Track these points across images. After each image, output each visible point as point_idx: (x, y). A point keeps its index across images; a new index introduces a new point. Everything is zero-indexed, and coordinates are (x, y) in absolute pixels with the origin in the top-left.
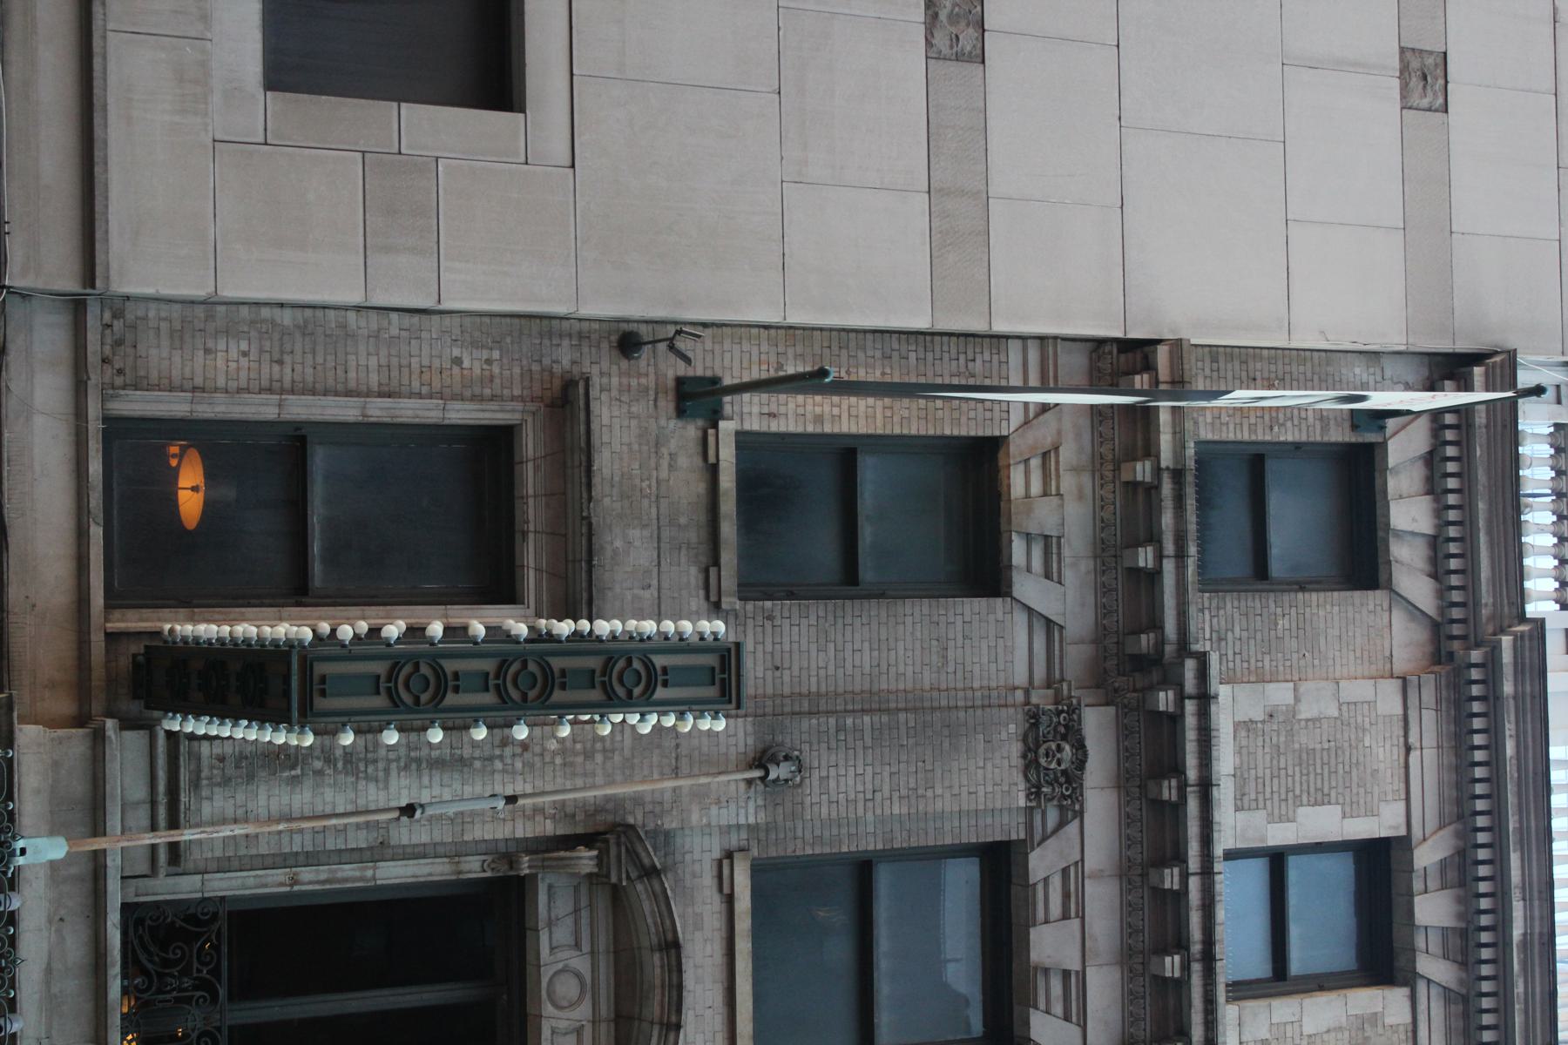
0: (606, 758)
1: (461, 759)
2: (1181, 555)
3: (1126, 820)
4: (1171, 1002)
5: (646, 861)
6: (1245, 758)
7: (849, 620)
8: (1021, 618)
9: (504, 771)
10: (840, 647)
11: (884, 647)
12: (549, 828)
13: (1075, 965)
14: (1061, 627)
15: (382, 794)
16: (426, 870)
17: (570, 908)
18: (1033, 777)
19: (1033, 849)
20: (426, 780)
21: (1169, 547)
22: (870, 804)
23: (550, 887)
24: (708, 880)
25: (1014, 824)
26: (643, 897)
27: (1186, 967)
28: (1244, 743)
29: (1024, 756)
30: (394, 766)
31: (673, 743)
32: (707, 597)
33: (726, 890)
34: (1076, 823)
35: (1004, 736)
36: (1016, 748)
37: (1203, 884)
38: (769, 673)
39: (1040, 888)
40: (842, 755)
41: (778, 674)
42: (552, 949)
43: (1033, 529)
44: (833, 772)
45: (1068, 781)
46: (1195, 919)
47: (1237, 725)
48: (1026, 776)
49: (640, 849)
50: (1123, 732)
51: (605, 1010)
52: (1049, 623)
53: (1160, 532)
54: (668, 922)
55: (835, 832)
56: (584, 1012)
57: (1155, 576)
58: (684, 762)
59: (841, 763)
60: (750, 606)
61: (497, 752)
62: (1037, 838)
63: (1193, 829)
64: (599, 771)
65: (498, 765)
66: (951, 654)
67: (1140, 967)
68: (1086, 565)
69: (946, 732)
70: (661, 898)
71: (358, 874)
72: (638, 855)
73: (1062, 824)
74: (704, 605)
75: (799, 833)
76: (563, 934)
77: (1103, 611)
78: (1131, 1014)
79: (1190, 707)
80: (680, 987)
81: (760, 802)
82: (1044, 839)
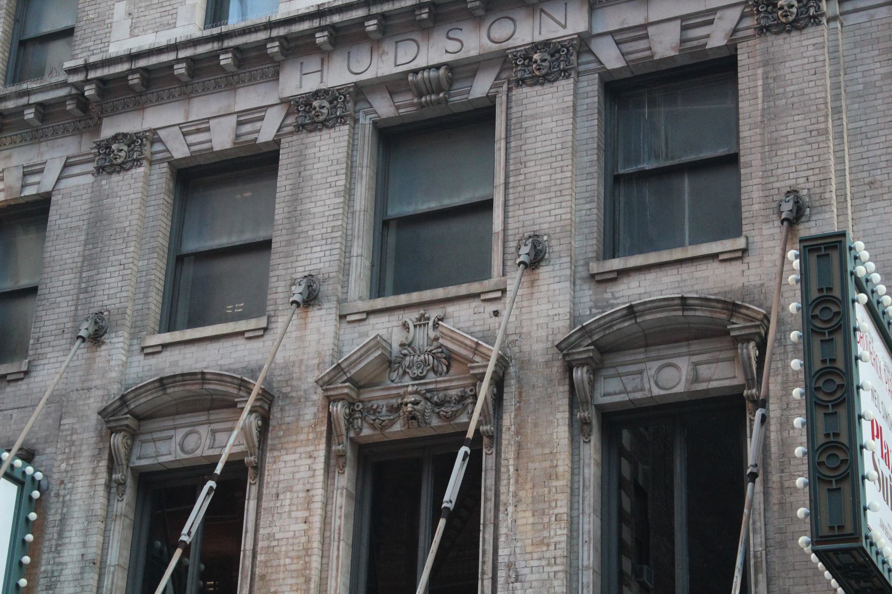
0: (76, 433)
1: (61, 520)
2: (28, 93)
3: (160, 101)
4: (253, 54)
5: (118, 404)
6: (149, 27)
7: (47, 291)
8: (64, 183)
9: (71, 494)
10: (59, 294)
11: (64, 267)
12: (104, 463)
13: (233, 119)
14: (68, 158)
15: (70, 566)
16: (116, 534)
17: (152, 444)
18: (129, 165)
19: (172, 157)
20: (67, 540)
21: (24, 101)
22: (126, 266)
23: (139, 458)
24: (153, 361)
25: (158, 171)
26: (137, 403)
27: (225, 50)
28: (141, 29)
29: (119, 172)
30: (57, 560)
31: (75, 393)
32: (22, 379)
33: (159, 349)
34: (159, 132)
35: (107, 187)
36: (115, 178)
37: (183, 48)
38: (65, 336)
39: (193, 148)
40: (99, 288)
41: (66, 330)
42: (170, 454)
43: (19, 184)
44: (106, 292)
45: (134, 142)
46: (202, 49)
47: (132, 36)
48: (129, 169)
49: (111, 409)
50: (115, 111)
51: (203, 418)
52: (66, 166)
53: (17, 107)
54: (149, 387)
55: (143, 285)
56: (204, 430)
57: (40, 105)
58: (86, 385)
59: (102, 287)
60: (31, 352)
61: (61, 499)
62: (166, 155)
63: (154, 60)
64: (81, 436)
65: (67, 498)
66: (74, 224)
67: (236, 78)
68: (43, 147)
69: (99, 224)
70: (137, 392)
71: (111, 576)
72: (114, 410)
73: (160, 141)
74: (26, 381)
75: (140, 307)
76: (163, 447)
77: (66, 130)
78: (262, 78)
79: (92, 75)
80: (183, 375)
81: (113, 335)
82: (168, 150)
